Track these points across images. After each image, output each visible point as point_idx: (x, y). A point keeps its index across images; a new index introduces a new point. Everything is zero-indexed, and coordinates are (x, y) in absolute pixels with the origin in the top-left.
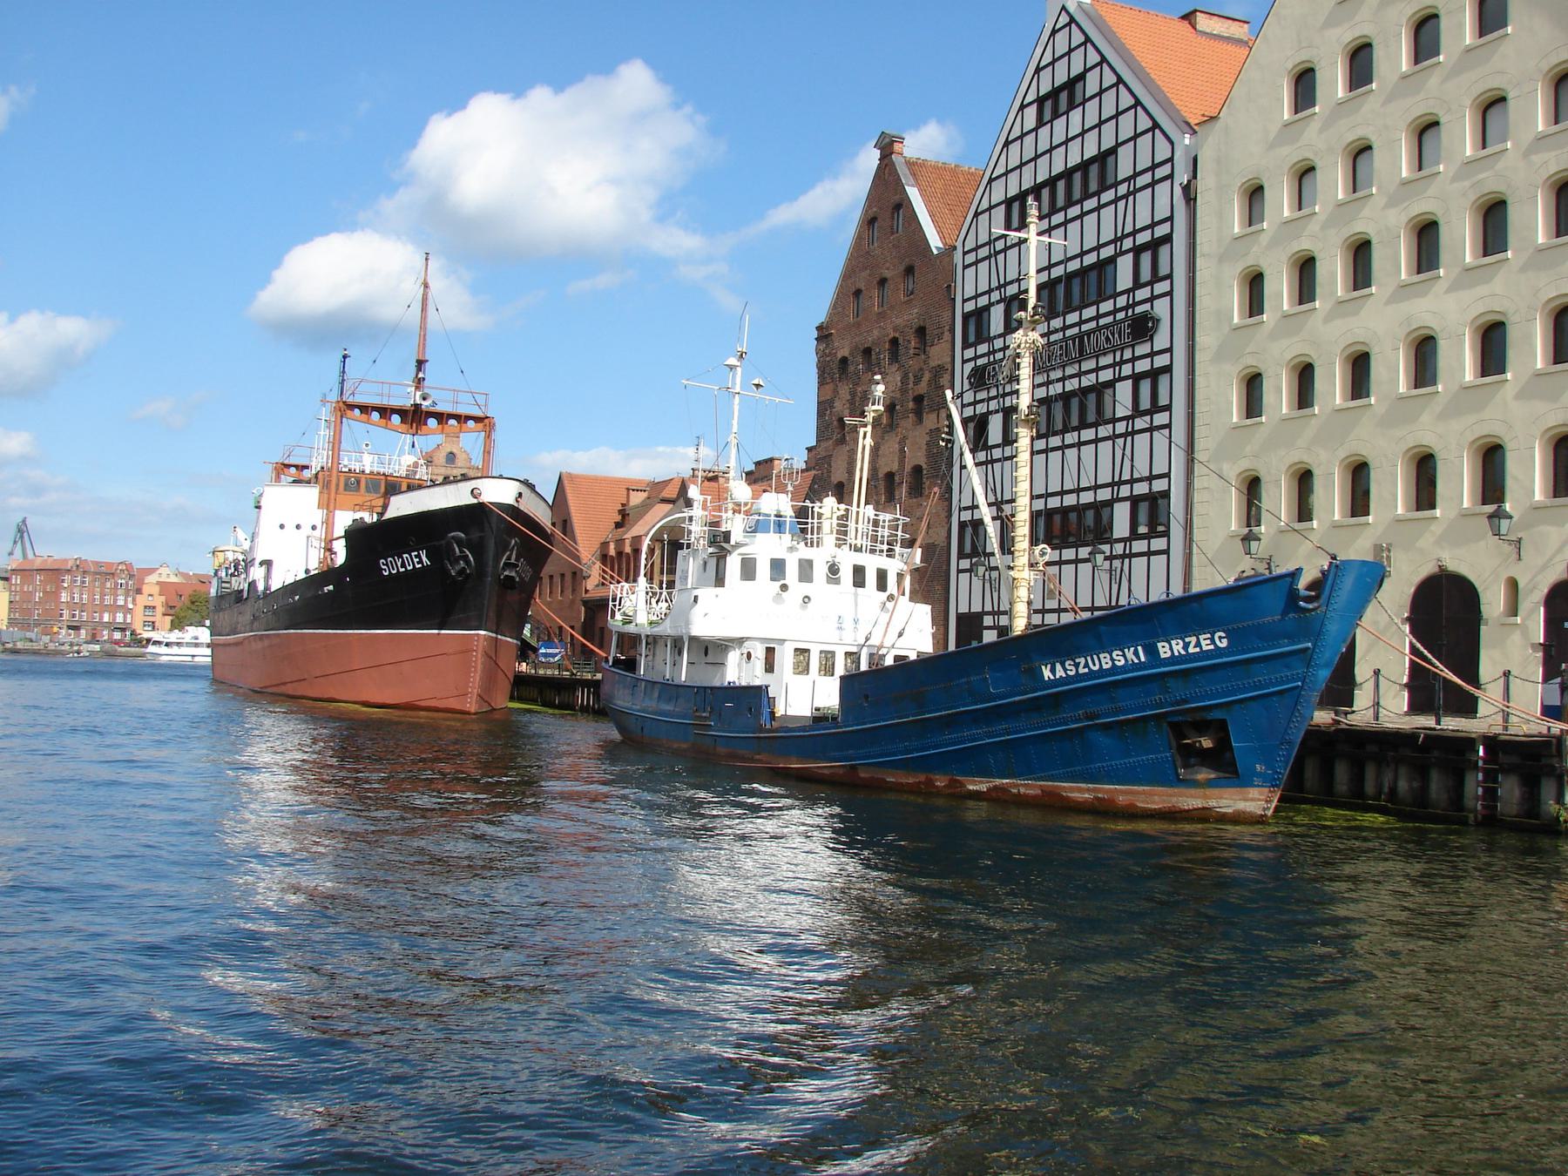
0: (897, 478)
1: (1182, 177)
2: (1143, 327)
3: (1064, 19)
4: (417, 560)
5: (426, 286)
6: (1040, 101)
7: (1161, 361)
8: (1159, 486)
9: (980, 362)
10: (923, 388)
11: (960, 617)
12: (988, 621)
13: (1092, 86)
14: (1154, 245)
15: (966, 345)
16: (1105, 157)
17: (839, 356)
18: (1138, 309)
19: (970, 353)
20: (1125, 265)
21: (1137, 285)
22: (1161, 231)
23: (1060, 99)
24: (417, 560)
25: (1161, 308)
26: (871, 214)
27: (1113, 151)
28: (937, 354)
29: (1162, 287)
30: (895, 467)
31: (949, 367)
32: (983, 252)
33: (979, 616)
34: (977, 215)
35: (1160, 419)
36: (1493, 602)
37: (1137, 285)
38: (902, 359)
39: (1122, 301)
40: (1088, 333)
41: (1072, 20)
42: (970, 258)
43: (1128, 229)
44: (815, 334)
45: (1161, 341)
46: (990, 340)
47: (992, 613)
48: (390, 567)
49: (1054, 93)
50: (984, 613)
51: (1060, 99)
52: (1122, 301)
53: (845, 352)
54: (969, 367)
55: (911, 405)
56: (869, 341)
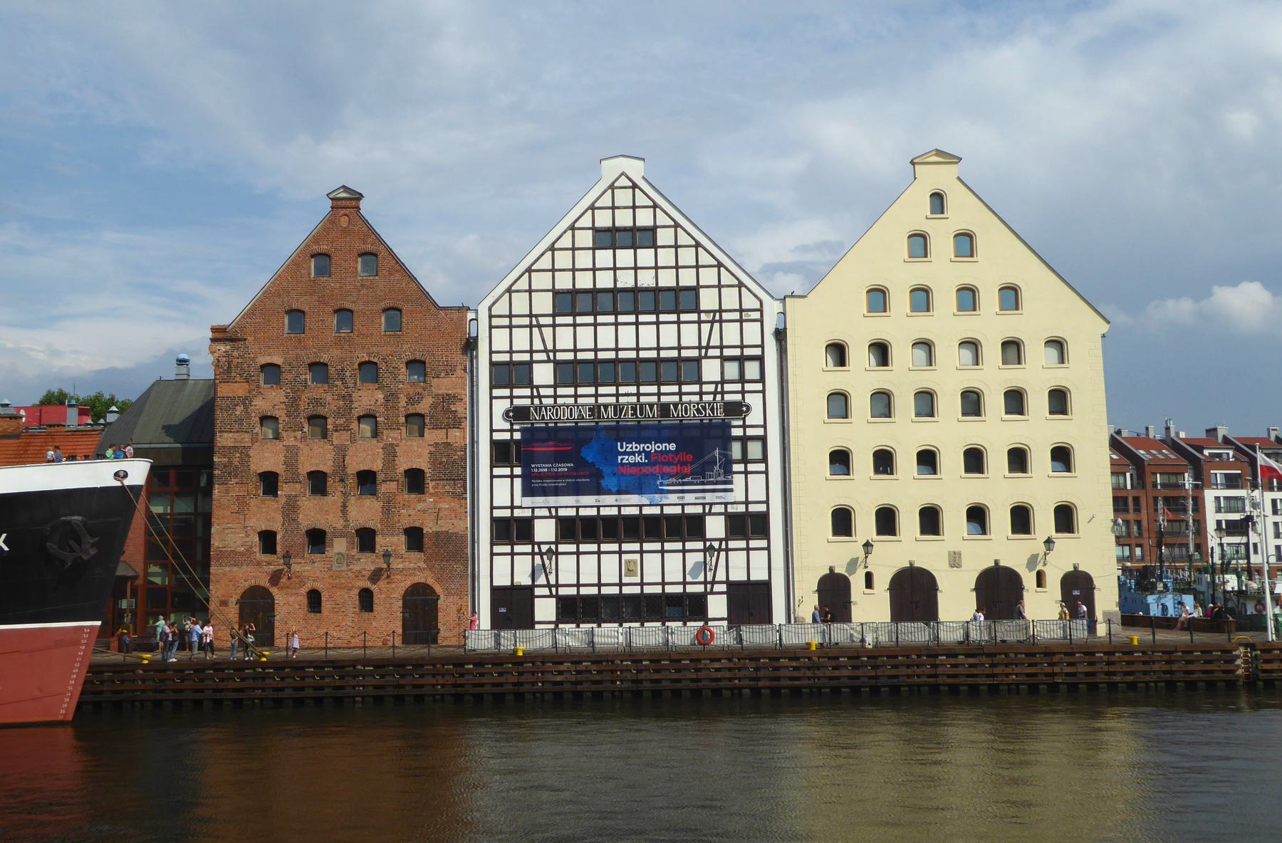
0: (380, 477)
1: (770, 325)
3: (623, 182)
6: (596, 231)
7: (750, 432)
8: (762, 508)
9: (517, 402)
10: (424, 407)
11: (495, 591)
12: (538, 591)
13: (664, 237)
14: (741, 360)
15: (492, 387)
17: (263, 360)
18: (728, 397)
19: (496, 392)
21: (723, 382)
25: (754, 400)
26: (316, 248)
27: (695, 290)
28: (442, 385)
29: (748, 387)
30: (377, 466)
31: (468, 399)
32: (526, 321)
33: (530, 589)
34: (509, 290)
36: (1029, 580)
37: (723, 382)
38: (386, 379)
39: (711, 388)
40: (676, 405)
41: (635, 186)
43: (715, 341)
44: (210, 335)
45: (754, 418)
46: (530, 384)
47: (549, 586)
49: (613, 230)
50: (532, 587)
52: (706, 388)
53: (277, 360)
54: (501, 406)
55: (403, 420)
56: (325, 358)
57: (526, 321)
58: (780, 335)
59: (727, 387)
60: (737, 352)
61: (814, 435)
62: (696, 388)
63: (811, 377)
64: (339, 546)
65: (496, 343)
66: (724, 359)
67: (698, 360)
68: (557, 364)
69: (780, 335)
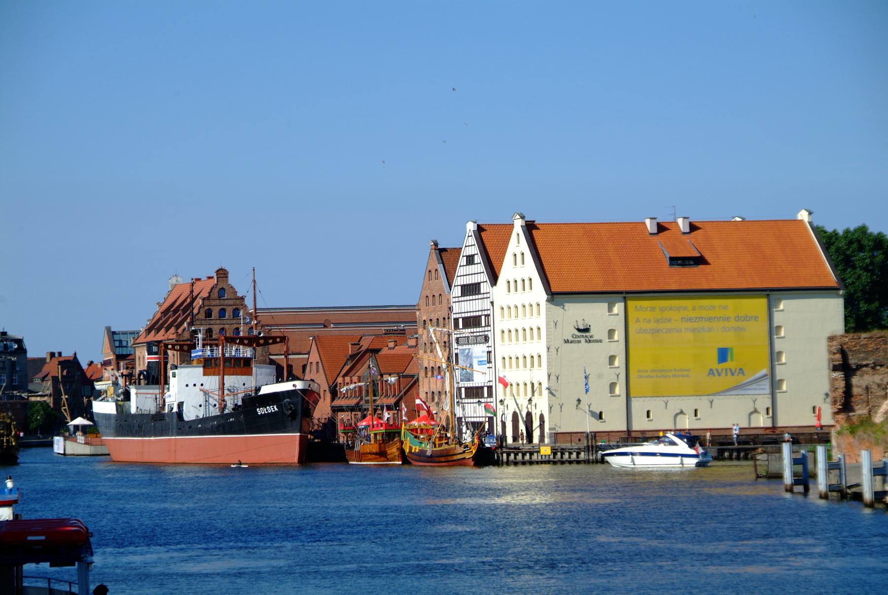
2: (486, 339)
4: (273, 409)
5: (254, 281)
6: (467, 257)
7: (490, 349)
8: (491, 384)
14: (488, 315)
16: (479, 284)
20: (483, 317)
22: (489, 312)
23: (470, 260)
24: (273, 409)
32: (457, 299)
35: (490, 365)
42: (454, 300)
45: (491, 343)
48: (261, 411)
51: (470, 260)
57: (457, 299)
58: (492, 303)
59: (486, 329)
60: (486, 313)
61: (502, 349)
62: (481, 329)
63: (500, 323)
64: (436, 400)
65: (456, 308)
66: (486, 316)
67: (480, 316)
68: (463, 318)
69: (492, 303)
